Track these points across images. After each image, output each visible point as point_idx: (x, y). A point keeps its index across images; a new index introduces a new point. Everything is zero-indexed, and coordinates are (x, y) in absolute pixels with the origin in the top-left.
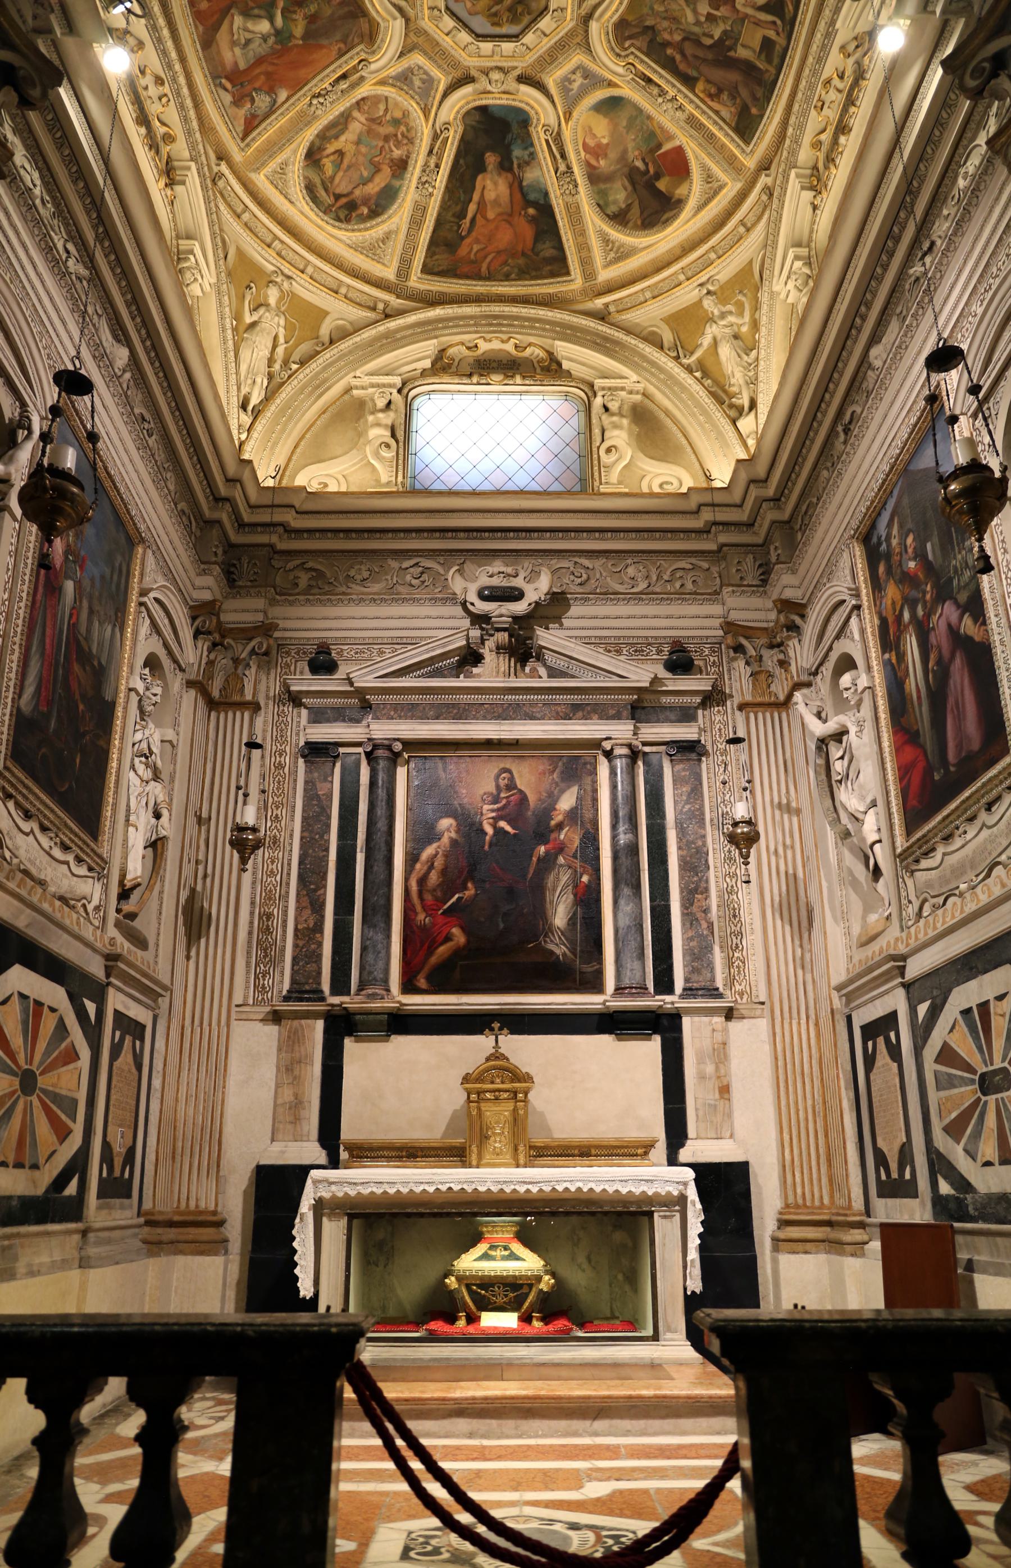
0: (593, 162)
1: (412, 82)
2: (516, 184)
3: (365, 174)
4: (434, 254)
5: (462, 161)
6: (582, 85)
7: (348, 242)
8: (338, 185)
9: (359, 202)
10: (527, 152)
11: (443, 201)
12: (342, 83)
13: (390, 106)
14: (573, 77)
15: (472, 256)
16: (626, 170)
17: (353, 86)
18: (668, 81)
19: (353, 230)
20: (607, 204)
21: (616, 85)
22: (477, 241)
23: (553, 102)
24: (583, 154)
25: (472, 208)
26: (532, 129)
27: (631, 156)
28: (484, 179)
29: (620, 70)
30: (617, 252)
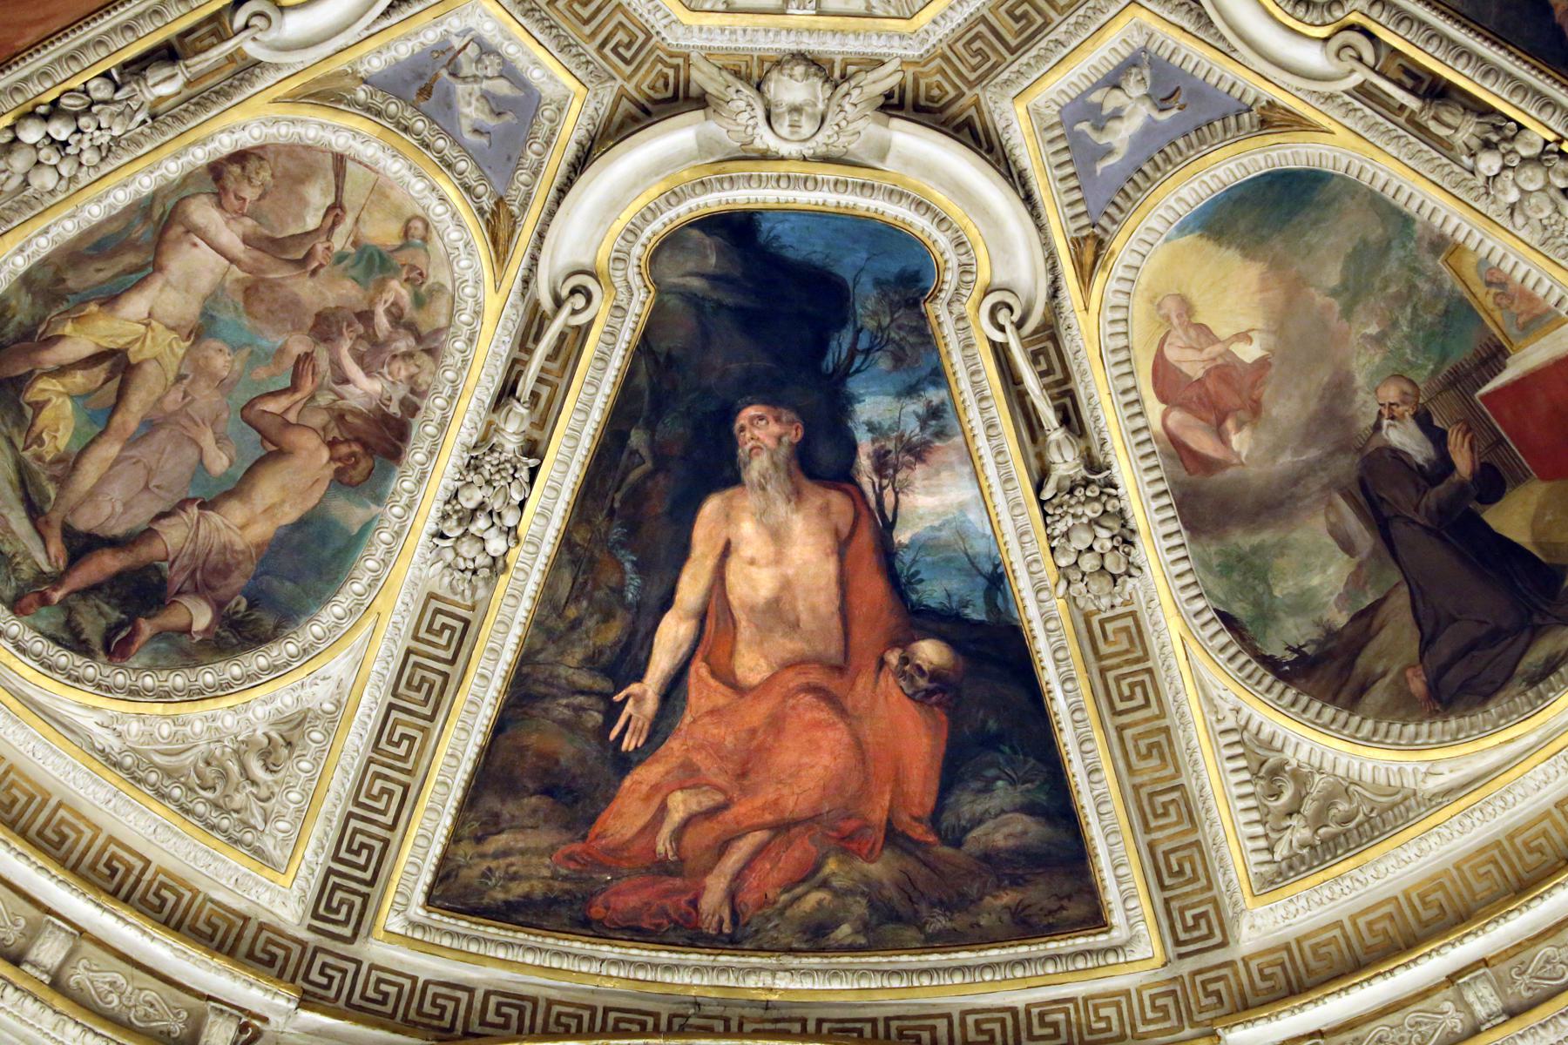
0: (1202, 442)
1: (448, 104)
2: (865, 538)
3: (219, 462)
4: (494, 825)
5: (637, 438)
6: (1149, 129)
7: (106, 739)
8: (92, 494)
9: (178, 579)
10: (916, 406)
11: (548, 601)
12: (155, 75)
13: (352, 197)
14: (1114, 100)
15: (663, 844)
16: (1346, 465)
17: (200, 98)
18: (1521, 88)
19: (134, 693)
20: (1266, 615)
21: (1293, 122)
22: (689, 777)
23: (1028, 199)
24: (1154, 409)
25: (673, 633)
26: (938, 310)
27: (1365, 407)
28: (728, 517)
29: (1312, 57)
30: (1319, 821)
